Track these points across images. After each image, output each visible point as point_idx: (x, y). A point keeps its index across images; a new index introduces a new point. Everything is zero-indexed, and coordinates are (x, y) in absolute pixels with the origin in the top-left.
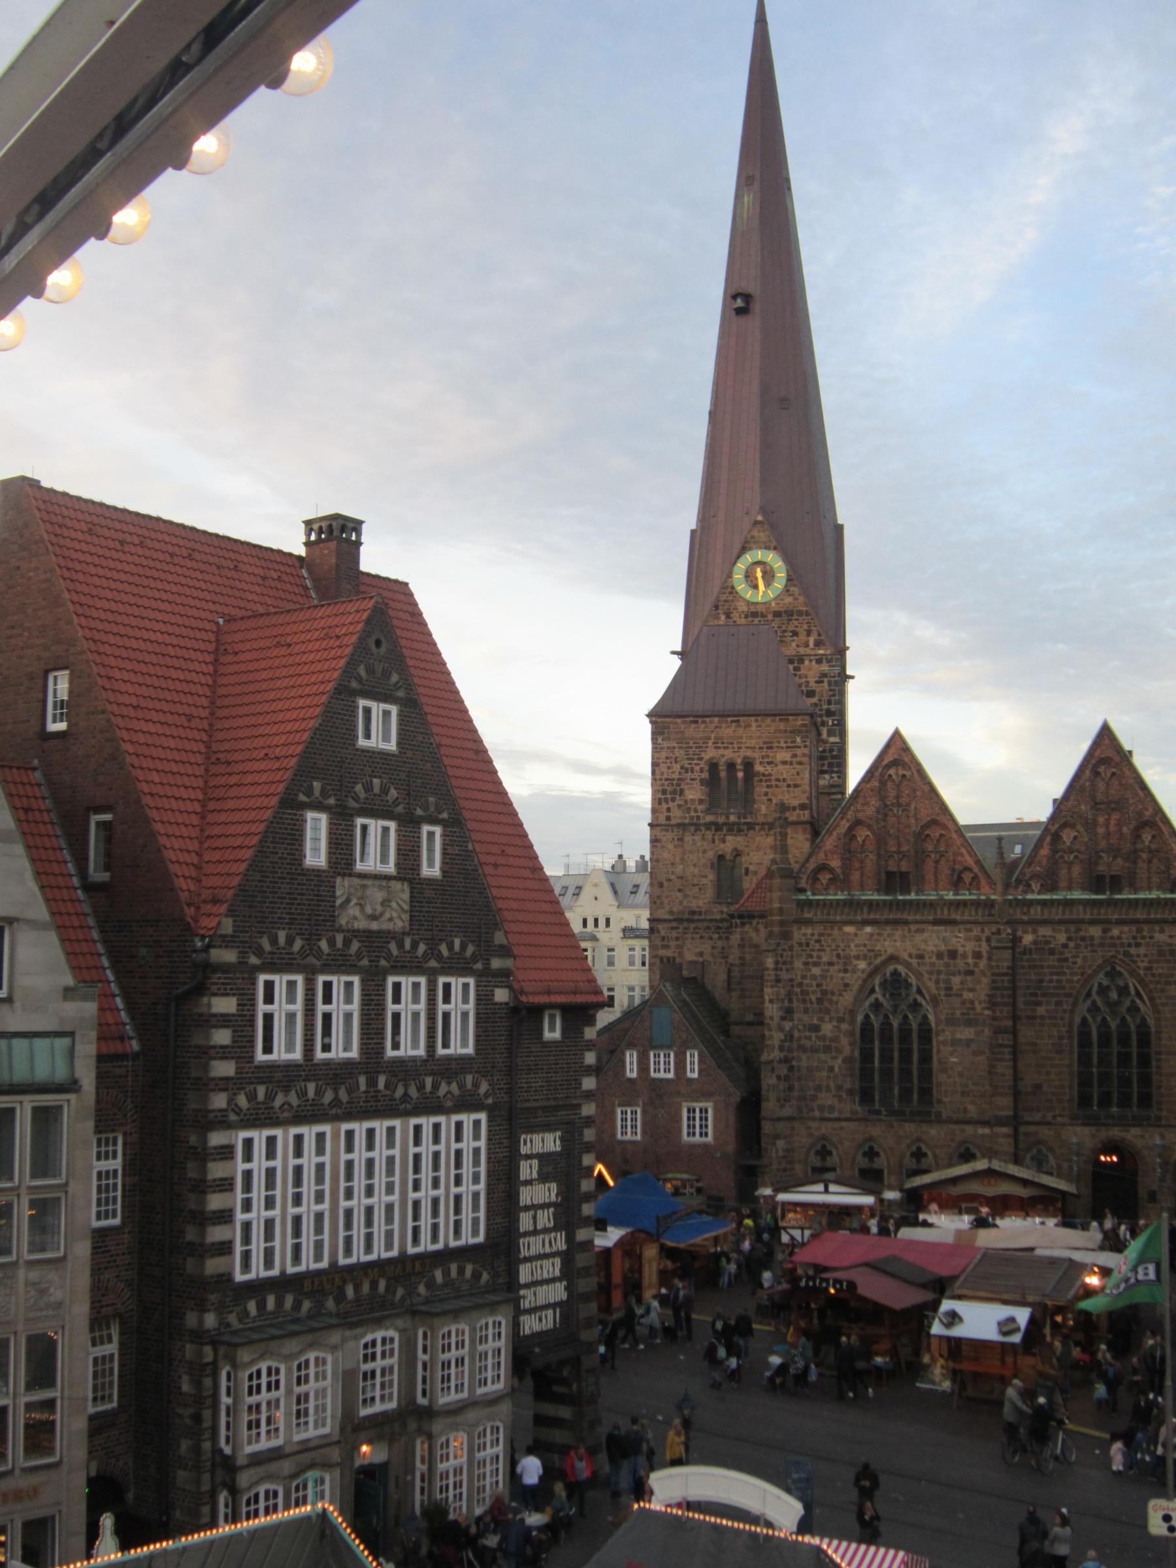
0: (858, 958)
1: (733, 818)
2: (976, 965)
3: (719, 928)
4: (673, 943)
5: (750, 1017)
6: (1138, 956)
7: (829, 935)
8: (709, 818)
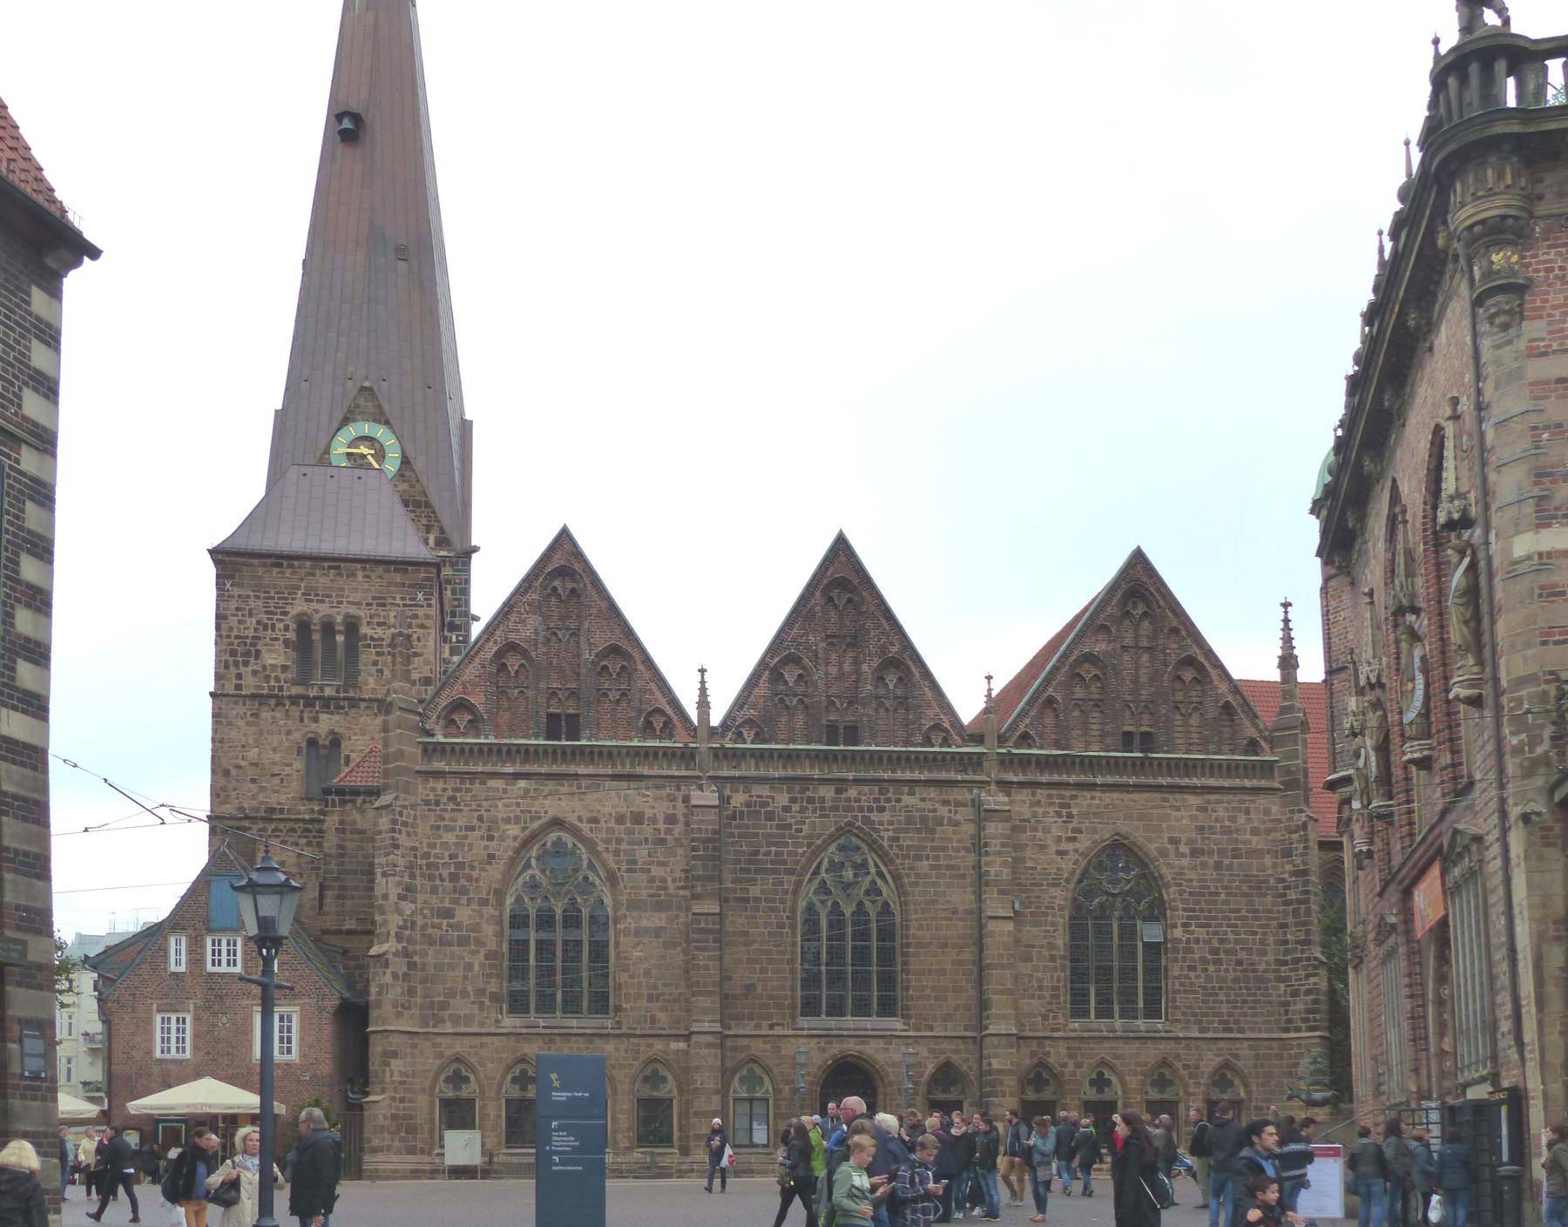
0: (507, 820)
1: (328, 692)
2: (669, 831)
5: (350, 924)
6: (881, 823)
7: (468, 790)
8: (296, 690)
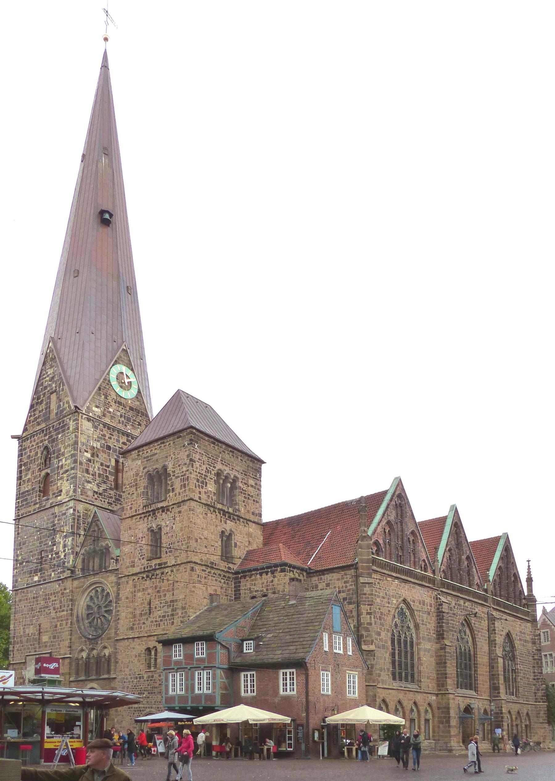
4: (203, 580)
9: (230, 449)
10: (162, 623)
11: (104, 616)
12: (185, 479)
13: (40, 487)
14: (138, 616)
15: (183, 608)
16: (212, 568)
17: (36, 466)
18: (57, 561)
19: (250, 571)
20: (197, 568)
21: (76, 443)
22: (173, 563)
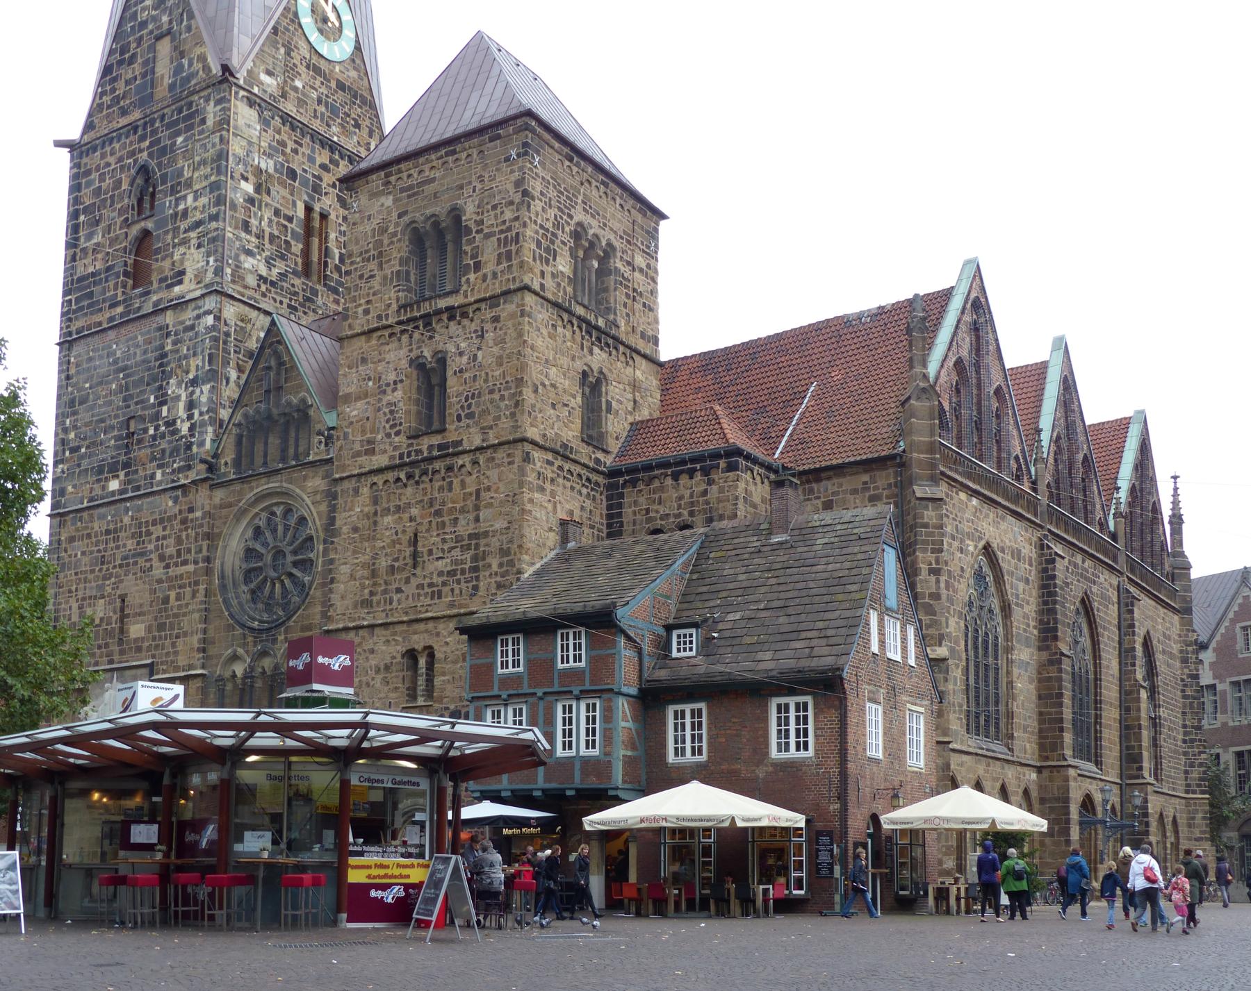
3: (588, 480)
4: (548, 486)
9: (601, 177)
10: (446, 589)
11: (290, 575)
12: (510, 243)
13: (126, 265)
14: (383, 571)
15: (504, 552)
16: (566, 458)
17: (116, 214)
18: (170, 442)
19: (648, 468)
20: (536, 455)
21: (222, 156)
22: (477, 442)
